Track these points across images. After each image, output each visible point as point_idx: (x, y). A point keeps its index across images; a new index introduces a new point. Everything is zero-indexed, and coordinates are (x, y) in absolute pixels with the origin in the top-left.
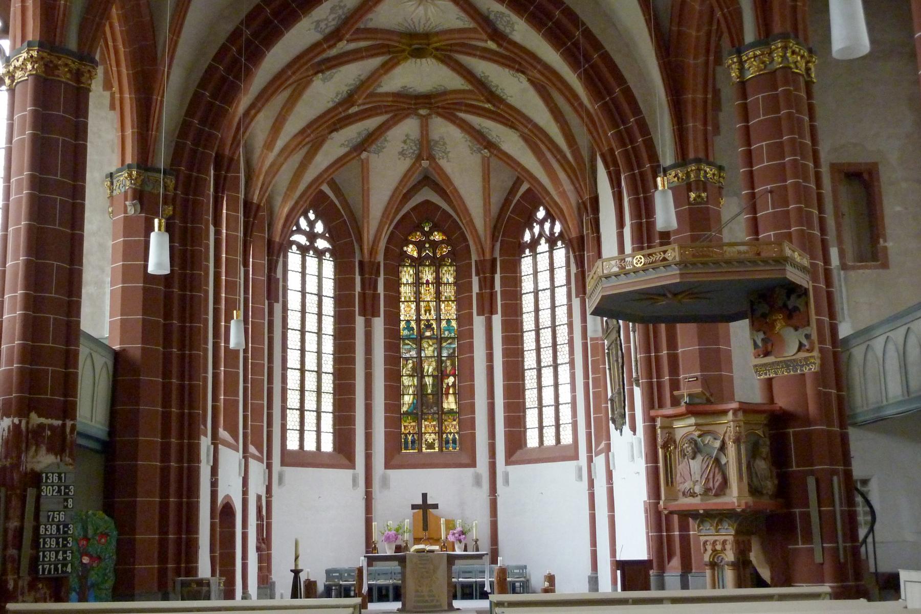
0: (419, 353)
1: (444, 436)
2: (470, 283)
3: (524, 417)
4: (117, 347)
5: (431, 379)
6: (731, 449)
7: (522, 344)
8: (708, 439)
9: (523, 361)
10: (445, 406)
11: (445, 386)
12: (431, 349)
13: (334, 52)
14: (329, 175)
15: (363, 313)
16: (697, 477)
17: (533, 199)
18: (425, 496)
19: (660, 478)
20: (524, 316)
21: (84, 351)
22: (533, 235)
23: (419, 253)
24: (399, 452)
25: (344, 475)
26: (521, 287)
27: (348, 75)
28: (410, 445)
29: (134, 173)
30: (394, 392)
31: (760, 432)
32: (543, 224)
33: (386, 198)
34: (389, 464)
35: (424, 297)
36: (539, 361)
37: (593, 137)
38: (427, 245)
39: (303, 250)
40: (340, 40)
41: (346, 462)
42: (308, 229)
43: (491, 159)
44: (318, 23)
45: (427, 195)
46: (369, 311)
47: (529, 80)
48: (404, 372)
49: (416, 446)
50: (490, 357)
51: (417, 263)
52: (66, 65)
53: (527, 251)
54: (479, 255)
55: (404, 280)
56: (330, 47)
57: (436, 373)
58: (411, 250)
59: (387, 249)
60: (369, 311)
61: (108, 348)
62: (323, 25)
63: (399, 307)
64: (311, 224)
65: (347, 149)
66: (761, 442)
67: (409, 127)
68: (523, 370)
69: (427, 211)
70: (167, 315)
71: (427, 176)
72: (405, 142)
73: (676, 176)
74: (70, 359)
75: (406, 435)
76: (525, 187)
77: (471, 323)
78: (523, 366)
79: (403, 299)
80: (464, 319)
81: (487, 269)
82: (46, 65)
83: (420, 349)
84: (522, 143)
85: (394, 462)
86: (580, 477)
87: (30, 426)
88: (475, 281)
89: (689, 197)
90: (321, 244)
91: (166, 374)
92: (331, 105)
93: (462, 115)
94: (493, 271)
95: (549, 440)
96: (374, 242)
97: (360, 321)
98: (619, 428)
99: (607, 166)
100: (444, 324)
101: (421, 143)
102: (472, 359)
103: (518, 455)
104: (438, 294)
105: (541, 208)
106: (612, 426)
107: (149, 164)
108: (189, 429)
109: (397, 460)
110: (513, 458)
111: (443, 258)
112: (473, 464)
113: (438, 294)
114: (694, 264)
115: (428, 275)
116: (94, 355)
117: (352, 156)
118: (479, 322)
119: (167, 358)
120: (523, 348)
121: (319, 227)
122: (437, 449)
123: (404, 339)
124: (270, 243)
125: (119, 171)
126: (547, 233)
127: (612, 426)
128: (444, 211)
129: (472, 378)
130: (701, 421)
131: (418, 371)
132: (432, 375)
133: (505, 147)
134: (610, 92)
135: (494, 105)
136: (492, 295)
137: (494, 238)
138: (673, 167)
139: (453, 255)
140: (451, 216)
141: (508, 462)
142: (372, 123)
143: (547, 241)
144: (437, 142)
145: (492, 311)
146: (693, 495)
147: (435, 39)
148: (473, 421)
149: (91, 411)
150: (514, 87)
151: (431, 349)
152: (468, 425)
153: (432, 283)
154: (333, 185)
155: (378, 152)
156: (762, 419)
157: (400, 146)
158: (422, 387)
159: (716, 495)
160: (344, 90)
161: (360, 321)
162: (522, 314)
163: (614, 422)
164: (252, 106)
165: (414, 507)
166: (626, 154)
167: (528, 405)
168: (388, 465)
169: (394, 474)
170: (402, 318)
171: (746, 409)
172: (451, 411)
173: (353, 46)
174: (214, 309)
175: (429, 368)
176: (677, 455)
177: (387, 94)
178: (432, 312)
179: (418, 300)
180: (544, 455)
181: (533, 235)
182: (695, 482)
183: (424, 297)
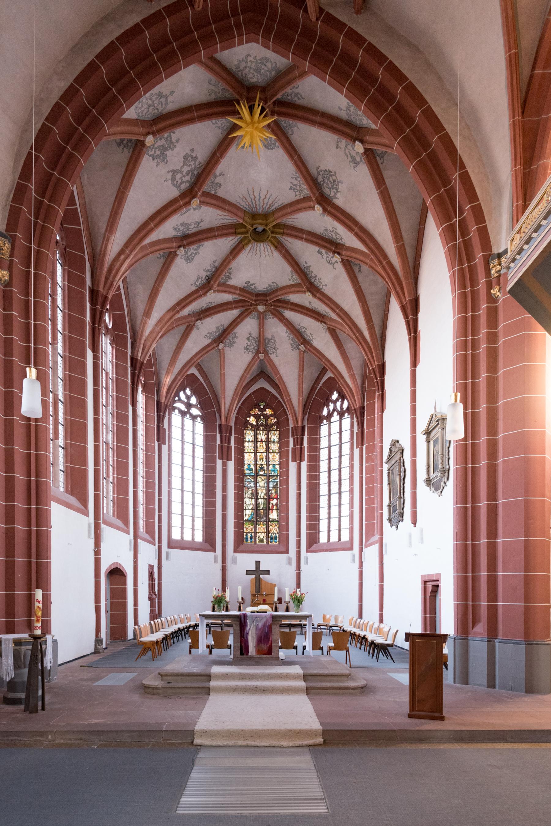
1: (270, 535)
2: (288, 442)
5: (263, 500)
7: (319, 480)
9: (319, 491)
10: (271, 516)
11: (271, 505)
12: (263, 482)
15: (221, 458)
22: (329, 410)
23: (257, 422)
25: (210, 555)
26: (320, 445)
28: (249, 539)
30: (240, 508)
34: (236, 550)
35: (260, 449)
36: (329, 490)
38: (262, 417)
41: (209, 547)
45: (262, 384)
48: (246, 496)
49: (253, 540)
50: (299, 488)
51: (256, 428)
54: (294, 422)
55: (247, 439)
57: (265, 497)
58: (252, 420)
63: (243, 456)
68: (319, 496)
69: (262, 393)
75: (247, 533)
77: (288, 466)
78: (319, 493)
79: (246, 451)
80: (284, 465)
83: (256, 482)
85: (239, 549)
86: (354, 560)
88: (291, 440)
94: (303, 434)
97: (219, 463)
103: (314, 547)
104: (268, 448)
109: (241, 548)
111: (271, 426)
113: (268, 448)
115: (262, 436)
118: (293, 466)
120: (319, 483)
122: (265, 543)
128: (273, 395)
131: (255, 495)
132: (263, 498)
136: (301, 449)
137: (304, 413)
139: (277, 424)
140: (277, 398)
141: (308, 551)
145: (301, 460)
148: (287, 525)
151: (263, 482)
153: (265, 441)
158: (257, 505)
161: (219, 463)
162: (319, 461)
168: (235, 551)
170: (245, 463)
172: (274, 520)
175: (262, 493)
178: (264, 460)
179: (256, 452)
180: (330, 548)
181: (329, 410)
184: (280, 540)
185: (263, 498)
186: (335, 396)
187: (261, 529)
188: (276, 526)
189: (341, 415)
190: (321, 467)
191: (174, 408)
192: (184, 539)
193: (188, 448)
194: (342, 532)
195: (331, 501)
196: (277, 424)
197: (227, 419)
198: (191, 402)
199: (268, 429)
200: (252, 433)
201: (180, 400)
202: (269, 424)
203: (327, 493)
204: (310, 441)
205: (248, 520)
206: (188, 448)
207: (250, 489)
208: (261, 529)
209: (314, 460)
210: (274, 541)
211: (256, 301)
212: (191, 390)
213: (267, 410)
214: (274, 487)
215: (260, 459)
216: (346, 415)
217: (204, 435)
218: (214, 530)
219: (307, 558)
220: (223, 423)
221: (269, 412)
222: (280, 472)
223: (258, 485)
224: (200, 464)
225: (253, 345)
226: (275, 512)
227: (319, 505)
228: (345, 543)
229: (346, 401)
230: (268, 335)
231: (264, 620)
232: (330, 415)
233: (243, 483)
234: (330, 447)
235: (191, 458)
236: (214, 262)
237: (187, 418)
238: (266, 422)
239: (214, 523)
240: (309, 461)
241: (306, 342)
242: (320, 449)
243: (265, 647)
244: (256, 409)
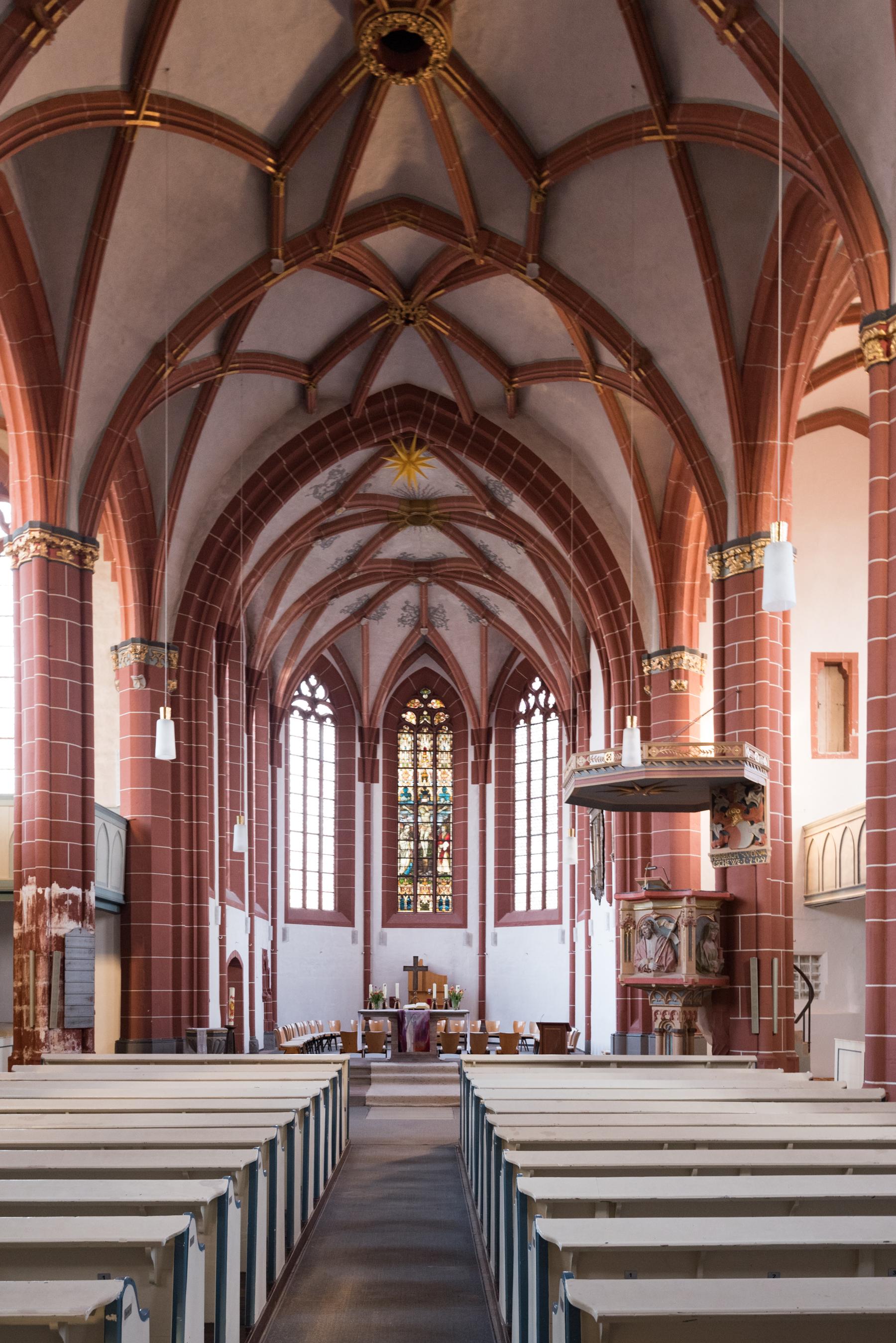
0: (416, 818)
1: (438, 898)
2: (466, 752)
3: (513, 882)
4: (128, 817)
5: (427, 843)
6: (684, 932)
7: (514, 812)
8: (663, 922)
9: (514, 829)
10: (439, 869)
11: (439, 851)
12: (428, 814)
13: (332, 518)
14: (331, 640)
15: (363, 779)
16: (652, 955)
17: (529, 670)
18: (416, 958)
19: (626, 951)
20: (517, 785)
21: (98, 823)
22: (528, 706)
23: (418, 720)
24: (394, 913)
26: (514, 757)
27: (347, 541)
28: (406, 905)
29: (139, 647)
31: (712, 918)
32: (538, 696)
33: (385, 665)
34: (386, 923)
35: (423, 763)
37: (587, 616)
38: (425, 713)
39: (305, 715)
40: (339, 506)
41: (345, 919)
42: (309, 695)
43: (489, 628)
44: (317, 487)
45: (426, 662)
46: (368, 776)
47: (527, 552)
48: (401, 836)
49: (412, 906)
50: (483, 825)
51: (416, 730)
52: (69, 547)
53: (522, 721)
54: (475, 725)
55: (402, 747)
56: (329, 514)
57: (431, 838)
58: (410, 717)
59: (386, 716)
60: (368, 776)
61: (119, 818)
62: (321, 491)
63: (396, 774)
64: (313, 690)
65: (347, 615)
66: (711, 925)
67: (408, 594)
68: (514, 838)
69: (425, 679)
70: (175, 787)
71: (426, 645)
72: (404, 609)
73: (660, 663)
74: (86, 834)
75: (402, 896)
76: (521, 657)
78: (514, 833)
79: (401, 766)
80: (460, 788)
81: (482, 739)
82: (49, 546)
83: (417, 815)
84: (519, 614)
87: (53, 896)
88: (471, 750)
89: (670, 685)
90: (323, 710)
91: (176, 842)
92: (330, 571)
93: (461, 583)
94: (489, 741)
95: (536, 905)
96: (373, 711)
97: (359, 787)
99: (598, 646)
100: (440, 791)
101: (420, 611)
102: (466, 825)
103: (507, 917)
104: (435, 761)
105: (537, 679)
106: (592, 896)
107: (153, 639)
108: (198, 894)
109: (394, 919)
110: (502, 920)
111: (440, 726)
112: (464, 925)
113: (435, 761)
114: (660, 762)
115: (425, 742)
116: (107, 824)
117: (352, 623)
118: (473, 790)
119: (176, 826)
120: (514, 817)
121: (321, 693)
122: (431, 910)
123: (401, 805)
124: (273, 708)
125: (124, 644)
126: (542, 704)
127: (592, 896)
128: (443, 680)
129: (465, 844)
130: (658, 905)
131: (415, 836)
132: (428, 840)
133: (503, 617)
134: (602, 574)
135: (492, 576)
136: (487, 764)
137: (490, 709)
138: (658, 654)
140: (449, 685)
141: (496, 925)
142: (371, 590)
143: (541, 713)
144: (436, 610)
145: (486, 780)
146: (647, 970)
147: (434, 506)
148: (465, 884)
149: (108, 878)
150: (513, 559)
151: (428, 814)
152: (460, 888)
153: (430, 751)
154: (334, 650)
155: (378, 618)
156: (714, 905)
157: (399, 613)
158: (417, 851)
159: (668, 972)
160: (344, 555)
161: (359, 787)
162: (514, 783)
163: (594, 892)
164: (252, 574)
165: (406, 968)
166: (614, 638)
167: (517, 871)
168: (385, 924)
169: (389, 931)
170: (399, 784)
171: (702, 897)
172: (445, 875)
173: (351, 512)
174: (219, 777)
175: (425, 832)
176: (635, 936)
177: (386, 561)
178: (430, 779)
179: (416, 767)
180: (530, 919)
181: (528, 706)
182: (650, 960)
183: (423, 763)
184: (453, 906)
185: (428, 840)
186: (536, 685)
187: (424, 889)
188: (448, 883)
189: (546, 713)
190: (516, 793)
191: (293, 709)
192: (308, 907)
193: (313, 766)
194: (547, 895)
195: (532, 847)
196: (449, 723)
197: (372, 718)
198: (317, 696)
200: (410, 738)
201: (301, 696)
202: (436, 723)
203: (526, 834)
204: (499, 752)
205: (403, 876)
206: (313, 766)
207: (407, 827)
210: (444, 907)
211: (415, 571)
212: (317, 678)
213: (434, 701)
214: (446, 822)
215: (423, 779)
216: (553, 715)
217: (336, 745)
218: (352, 893)
219: (495, 935)
220: (366, 725)
221: (436, 704)
222: (454, 799)
223: (419, 820)
224: (330, 790)
225: (411, 615)
226: (445, 862)
227: (514, 852)
228: (552, 912)
229: (551, 695)
230: (434, 603)
231: (422, 1017)
232: (530, 713)
233: (397, 817)
234: (529, 763)
235: (318, 781)
236: (359, 541)
237: (312, 723)
238: (432, 721)
239: (351, 881)
240: (498, 783)
242: (514, 764)
243: (423, 1044)
244: (417, 701)
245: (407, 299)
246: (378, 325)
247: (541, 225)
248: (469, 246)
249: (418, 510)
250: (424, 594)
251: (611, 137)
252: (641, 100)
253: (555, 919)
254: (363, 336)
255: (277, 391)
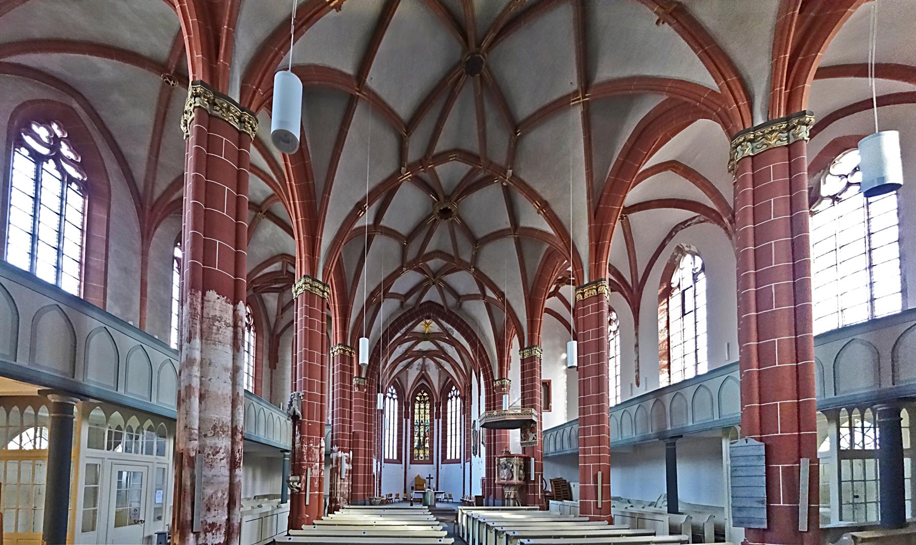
32: (454, 392)
51: (420, 402)
58: (418, 398)
67: (420, 361)
71: (423, 376)
80: (432, 420)
98: (475, 455)
115: (422, 406)
118: (436, 421)
131: (419, 435)
150: (451, 351)
152: (431, 452)
175: (422, 434)
187: (421, 452)
199: (425, 402)
208: (421, 452)
209: (445, 418)
221: (425, 394)
241: (442, 367)
245: (434, 277)
246: (425, 284)
247: (475, 258)
248: (454, 264)
249: (426, 337)
250: (424, 361)
251: (499, 235)
252: (509, 226)
253: (459, 461)
254: (420, 288)
255: (396, 303)
